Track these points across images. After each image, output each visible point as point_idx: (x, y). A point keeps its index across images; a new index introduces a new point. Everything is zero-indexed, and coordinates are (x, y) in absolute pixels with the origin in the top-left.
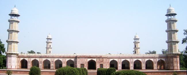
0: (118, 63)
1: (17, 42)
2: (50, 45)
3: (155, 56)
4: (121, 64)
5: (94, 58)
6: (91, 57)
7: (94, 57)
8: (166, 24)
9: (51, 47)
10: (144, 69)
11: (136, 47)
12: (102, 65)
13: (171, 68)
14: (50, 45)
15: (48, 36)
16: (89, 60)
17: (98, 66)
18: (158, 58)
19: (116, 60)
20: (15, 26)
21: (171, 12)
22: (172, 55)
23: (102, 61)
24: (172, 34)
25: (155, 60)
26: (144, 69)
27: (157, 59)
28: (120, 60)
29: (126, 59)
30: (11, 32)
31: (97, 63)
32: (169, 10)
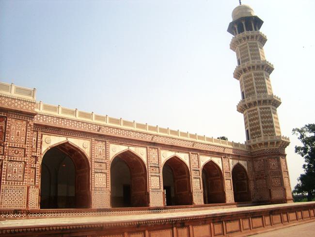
0: (94, 166)
3: (225, 148)
4: (108, 171)
10: (101, 212)
13: (276, 195)
18: (236, 156)
19: (81, 144)
22: (270, 147)
24: (264, 79)
25: (225, 161)
26: (157, 209)
27: (231, 160)
28: (100, 146)
29: (132, 149)
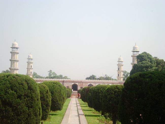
1: (18, 69)
2: (31, 66)
5: (77, 82)
6: (74, 81)
7: (76, 81)
8: (132, 58)
9: (32, 68)
11: (119, 70)
12: (81, 87)
14: (31, 66)
15: (29, 56)
16: (73, 83)
17: (79, 88)
20: (17, 57)
21: (135, 49)
23: (82, 85)
30: (14, 61)
31: (78, 86)
32: (134, 48)
